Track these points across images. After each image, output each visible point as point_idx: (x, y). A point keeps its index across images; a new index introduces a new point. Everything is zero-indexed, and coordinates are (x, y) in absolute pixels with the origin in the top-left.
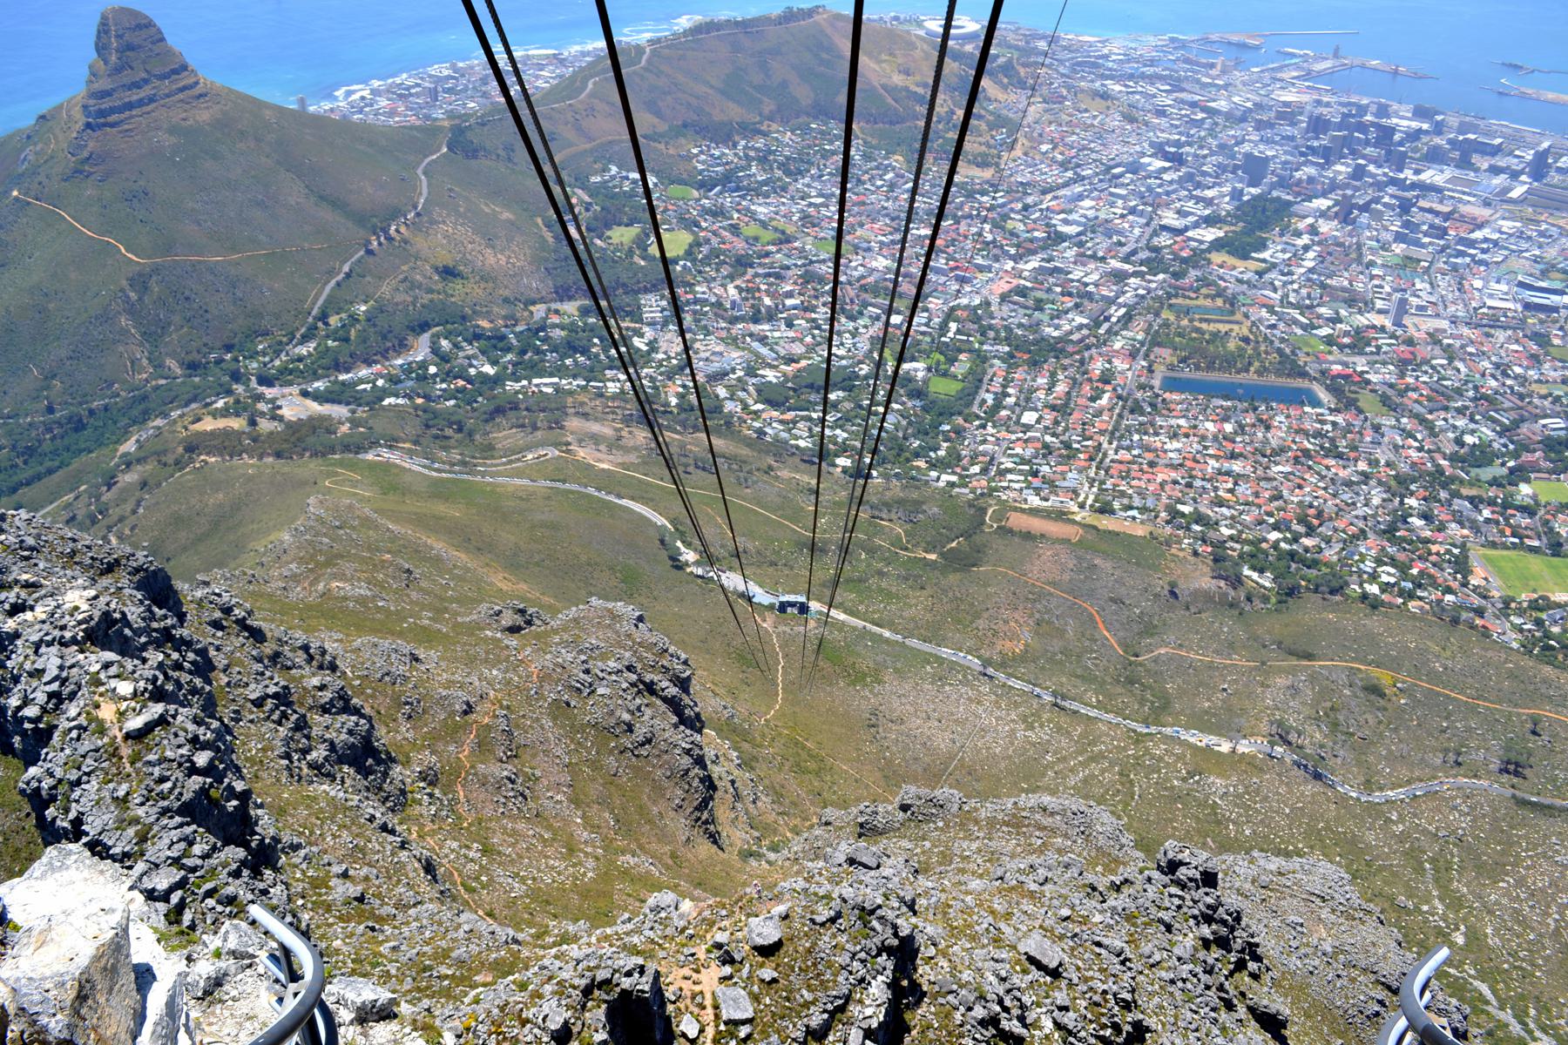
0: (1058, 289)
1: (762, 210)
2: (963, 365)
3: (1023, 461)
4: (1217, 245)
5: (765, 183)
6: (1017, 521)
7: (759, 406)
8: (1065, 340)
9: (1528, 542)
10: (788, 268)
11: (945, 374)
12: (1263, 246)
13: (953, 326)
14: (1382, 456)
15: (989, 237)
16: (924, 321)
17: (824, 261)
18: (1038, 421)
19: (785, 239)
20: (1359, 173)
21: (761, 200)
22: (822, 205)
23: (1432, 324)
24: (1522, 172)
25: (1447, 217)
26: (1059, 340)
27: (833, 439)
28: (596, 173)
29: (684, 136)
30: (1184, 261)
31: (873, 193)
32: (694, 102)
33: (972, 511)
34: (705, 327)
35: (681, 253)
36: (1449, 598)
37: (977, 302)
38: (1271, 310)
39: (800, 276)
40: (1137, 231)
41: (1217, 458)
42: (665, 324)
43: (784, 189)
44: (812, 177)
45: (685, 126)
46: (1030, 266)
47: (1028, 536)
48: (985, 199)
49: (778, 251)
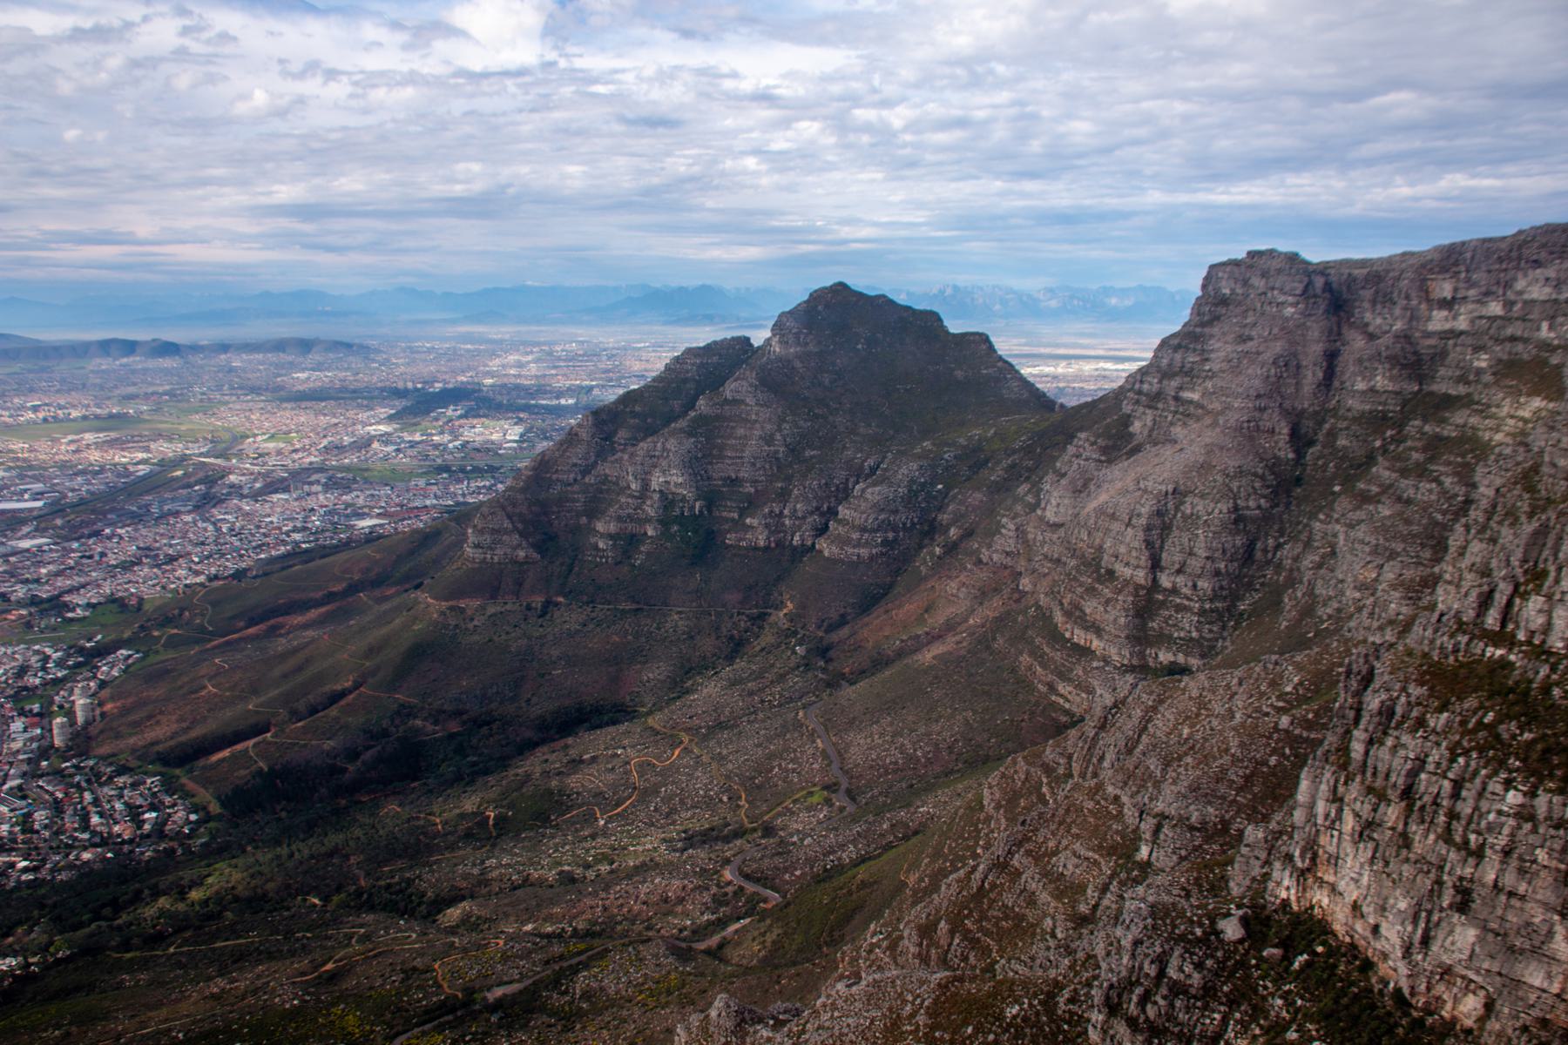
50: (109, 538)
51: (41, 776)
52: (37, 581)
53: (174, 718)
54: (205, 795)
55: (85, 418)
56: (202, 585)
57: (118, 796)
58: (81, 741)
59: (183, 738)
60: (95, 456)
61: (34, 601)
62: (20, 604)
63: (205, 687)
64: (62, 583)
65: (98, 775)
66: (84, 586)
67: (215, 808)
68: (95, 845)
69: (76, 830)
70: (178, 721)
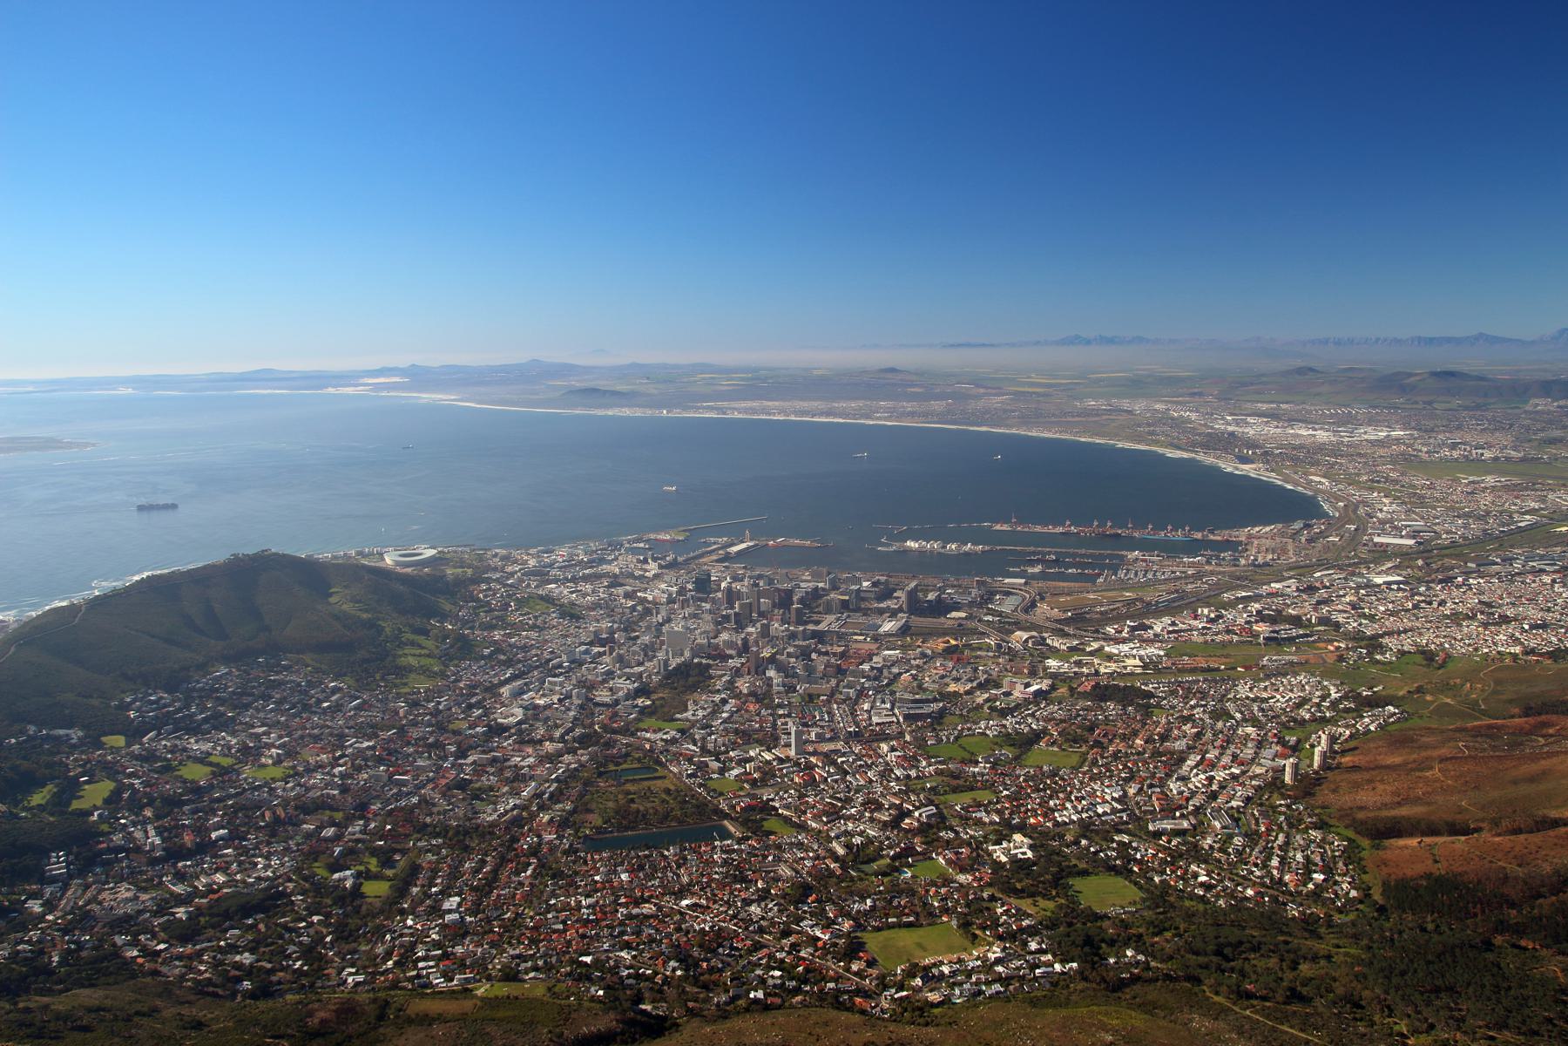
3: (437, 945)
4: (643, 711)
5: (206, 720)
6: (419, 1006)
7: (162, 946)
9: (905, 919)
10: (219, 800)
12: (686, 710)
14: (785, 871)
18: (460, 905)
19: (222, 772)
20: (765, 632)
22: (264, 733)
23: (827, 747)
24: (900, 610)
25: (843, 655)
26: (493, 825)
27: (238, 966)
30: (614, 732)
35: (99, 803)
36: (831, 985)
37: (415, 800)
38: (690, 760)
40: (572, 713)
41: (626, 905)
42: (70, 876)
46: (470, 759)
47: (426, 1020)
50: (1459, 587)
51: (1261, 805)
52: (1372, 618)
53: (1389, 788)
54: (1373, 879)
55: (1496, 459)
56: (1514, 656)
57: (1307, 845)
58: (1307, 785)
59: (1385, 813)
60: (1485, 500)
61: (1358, 637)
62: (1347, 636)
63: (1431, 768)
64: (1390, 623)
65: (1300, 821)
66: (1405, 631)
67: (1377, 896)
68: (1263, 885)
69: (1256, 865)
70: (1393, 793)
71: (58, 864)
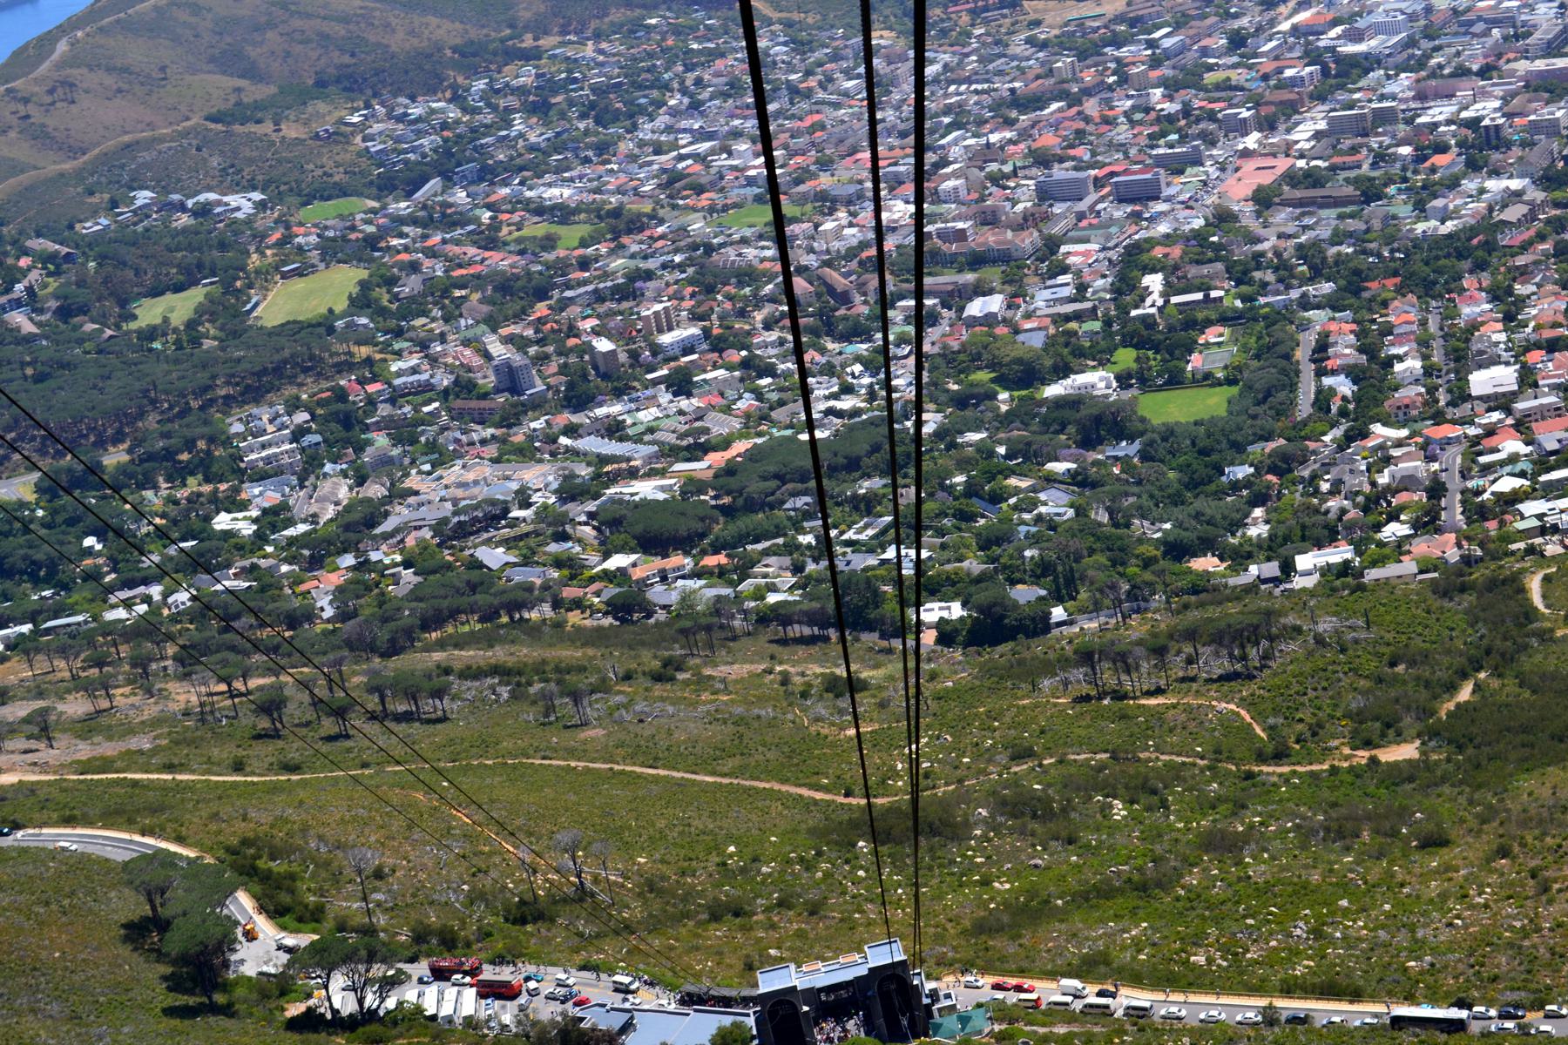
0: (1405, 150)
1: (556, 194)
2: (1215, 349)
8: (1488, 226)
10: (649, 275)
11: (1175, 380)
13: (1154, 282)
15: (1171, 107)
16: (1068, 291)
17: (744, 241)
21: (548, 178)
22: (712, 152)
28: (94, 213)
29: (324, 97)
31: (837, 106)
32: (339, 30)
33: (1469, 599)
34: (432, 446)
35: (341, 306)
39: (690, 281)
43: (604, 149)
44: (675, 113)
45: (321, 84)
48: (1124, 52)
49: (612, 252)
71: (267, 431)
